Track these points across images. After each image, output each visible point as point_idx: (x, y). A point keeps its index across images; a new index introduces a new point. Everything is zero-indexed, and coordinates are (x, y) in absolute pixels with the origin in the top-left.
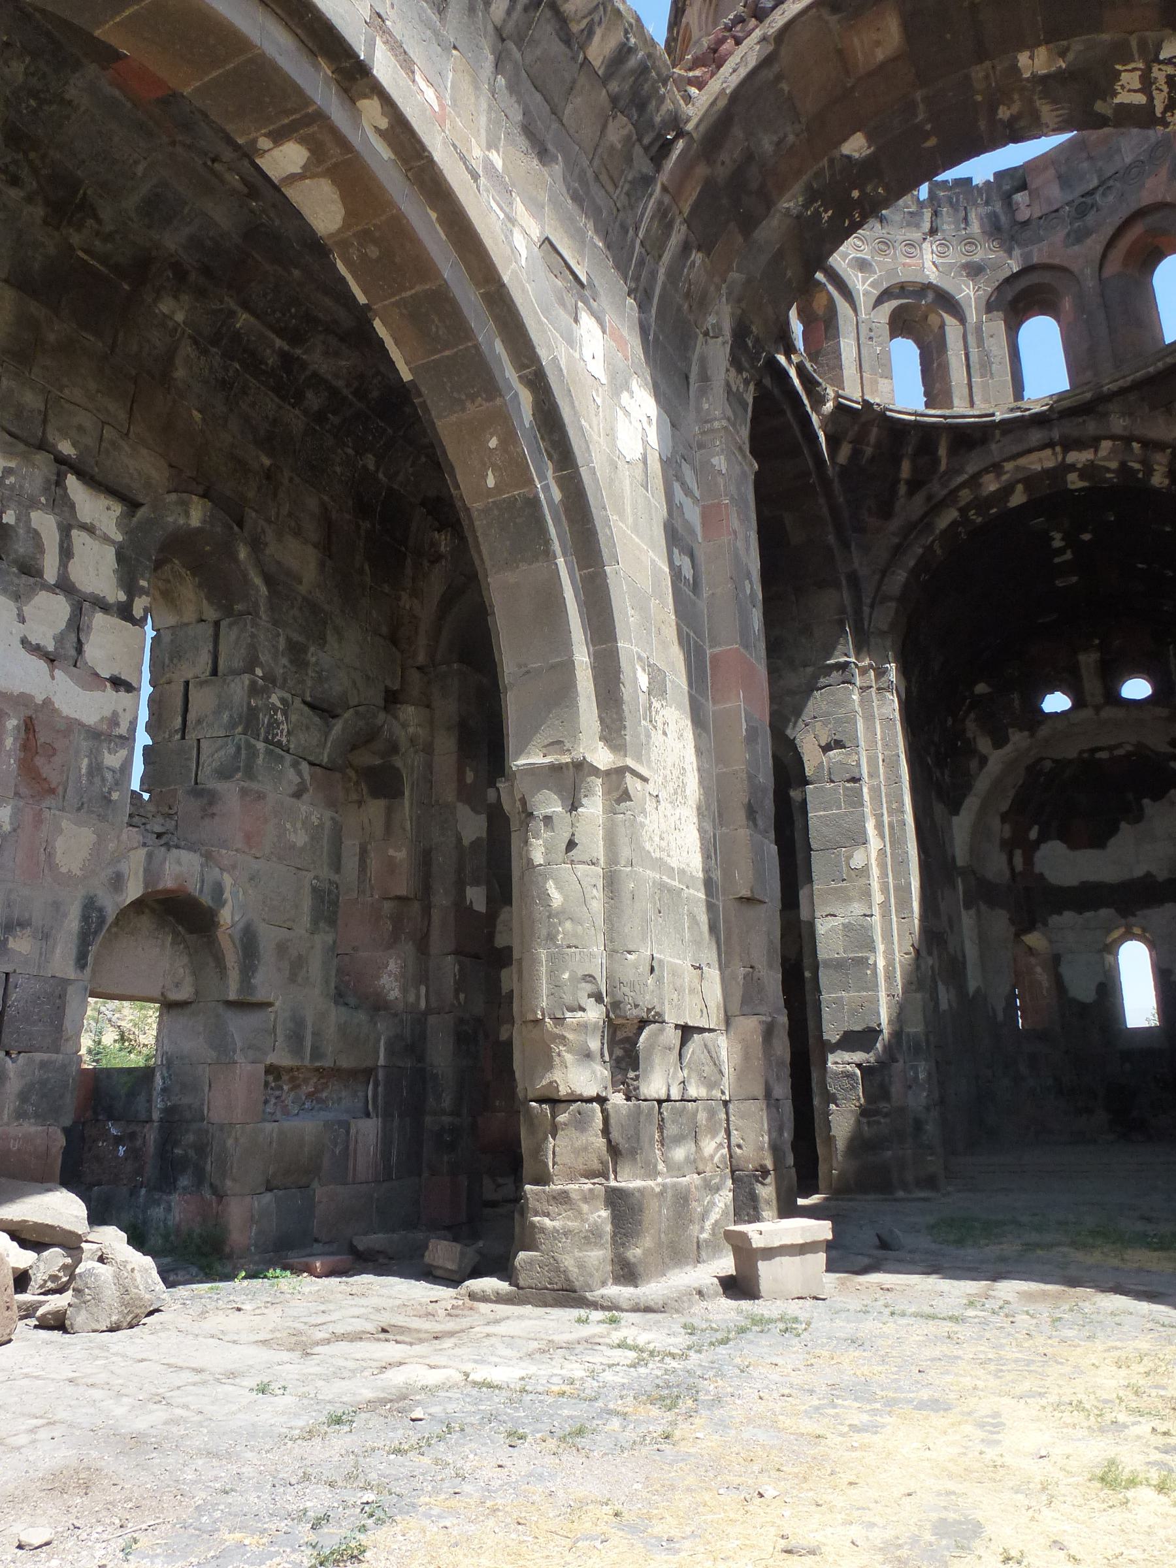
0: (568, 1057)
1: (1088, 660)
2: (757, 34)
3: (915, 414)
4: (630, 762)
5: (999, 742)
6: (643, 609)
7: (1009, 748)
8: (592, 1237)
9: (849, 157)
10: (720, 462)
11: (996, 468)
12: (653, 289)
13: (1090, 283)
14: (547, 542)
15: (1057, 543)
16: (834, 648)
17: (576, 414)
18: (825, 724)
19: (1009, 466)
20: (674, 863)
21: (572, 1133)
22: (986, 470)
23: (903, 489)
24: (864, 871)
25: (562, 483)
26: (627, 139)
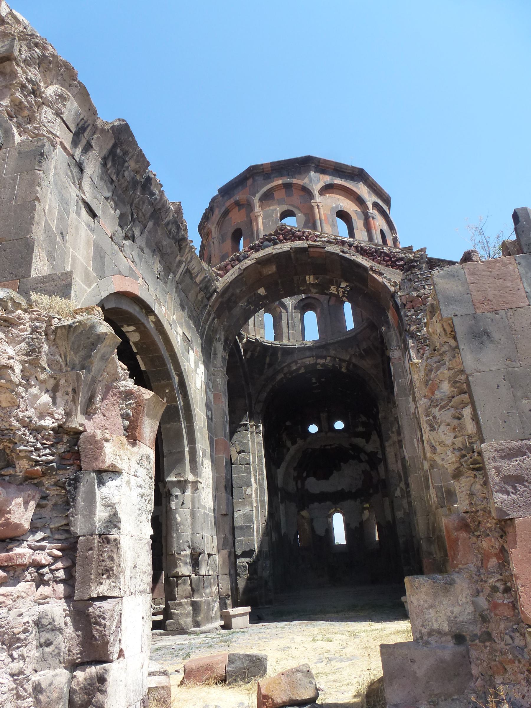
0: (181, 564)
1: (323, 416)
2: (238, 266)
3: (271, 343)
4: (199, 479)
5: (294, 443)
6: (201, 432)
7: (297, 445)
8: (188, 615)
9: (260, 294)
10: (219, 381)
11: (296, 362)
12: (204, 332)
13: (326, 306)
14: (180, 418)
15: (314, 380)
16: (243, 419)
17: (188, 381)
18: (239, 444)
19: (299, 362)
20: (207, 506)
21: (182, 586)
22: (293, 362)
23: (266, 366)
24: (250, 496)
25: (183, 400)
26: (203, 298)
